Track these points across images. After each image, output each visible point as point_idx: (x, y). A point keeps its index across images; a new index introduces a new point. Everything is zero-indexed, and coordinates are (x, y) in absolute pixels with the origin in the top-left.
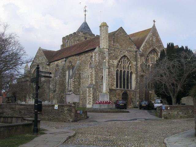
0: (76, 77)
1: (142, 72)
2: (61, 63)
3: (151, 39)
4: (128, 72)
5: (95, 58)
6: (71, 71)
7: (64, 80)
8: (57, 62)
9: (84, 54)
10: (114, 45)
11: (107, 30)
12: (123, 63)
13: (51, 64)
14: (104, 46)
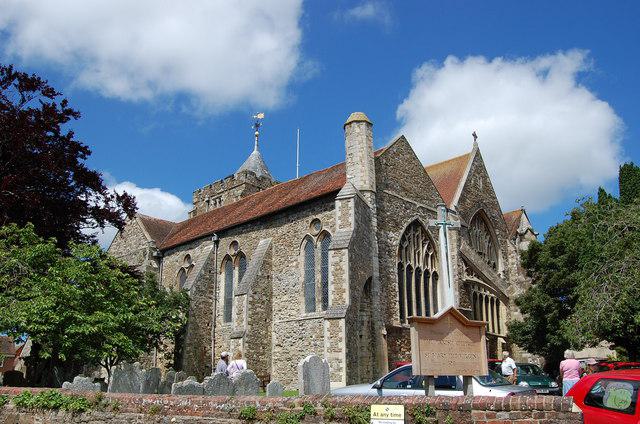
2: (202, 252)
6: (236, 273)
9: (284, 214)
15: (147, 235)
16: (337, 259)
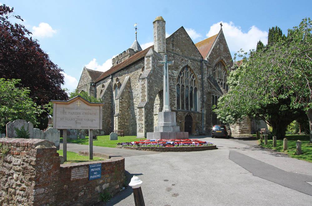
0: (124, 97)
1: (210, 88)
3: (218, 47)
7: (111, 102)
9: (133, 65)
10: (173, 50)
12: (185, 75)
13: (97, 84)
16: (143, 83)
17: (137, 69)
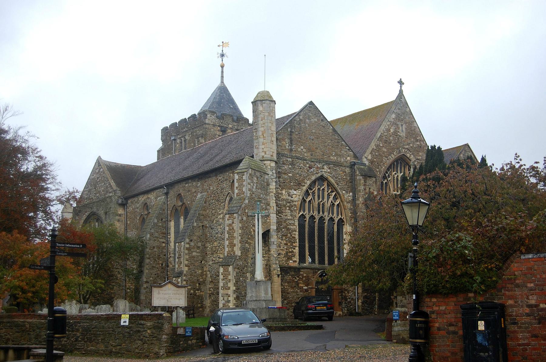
0: (195, 238)
3: (392, 131)
4: (332, 219)
5: (241, 186)
7: (164, 245)
8: (145, 197)
9: (214, 174)
10: (291, 150)
11: (272, 112)
12: (316, 197)
13: (129, 201)
14: (263, 154)
15: (113, 183)
16: (230, 222)
17: (222, 182)
